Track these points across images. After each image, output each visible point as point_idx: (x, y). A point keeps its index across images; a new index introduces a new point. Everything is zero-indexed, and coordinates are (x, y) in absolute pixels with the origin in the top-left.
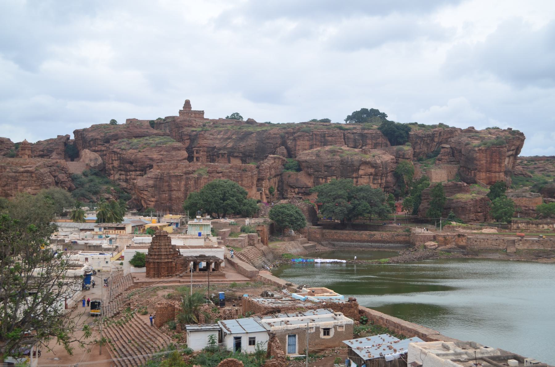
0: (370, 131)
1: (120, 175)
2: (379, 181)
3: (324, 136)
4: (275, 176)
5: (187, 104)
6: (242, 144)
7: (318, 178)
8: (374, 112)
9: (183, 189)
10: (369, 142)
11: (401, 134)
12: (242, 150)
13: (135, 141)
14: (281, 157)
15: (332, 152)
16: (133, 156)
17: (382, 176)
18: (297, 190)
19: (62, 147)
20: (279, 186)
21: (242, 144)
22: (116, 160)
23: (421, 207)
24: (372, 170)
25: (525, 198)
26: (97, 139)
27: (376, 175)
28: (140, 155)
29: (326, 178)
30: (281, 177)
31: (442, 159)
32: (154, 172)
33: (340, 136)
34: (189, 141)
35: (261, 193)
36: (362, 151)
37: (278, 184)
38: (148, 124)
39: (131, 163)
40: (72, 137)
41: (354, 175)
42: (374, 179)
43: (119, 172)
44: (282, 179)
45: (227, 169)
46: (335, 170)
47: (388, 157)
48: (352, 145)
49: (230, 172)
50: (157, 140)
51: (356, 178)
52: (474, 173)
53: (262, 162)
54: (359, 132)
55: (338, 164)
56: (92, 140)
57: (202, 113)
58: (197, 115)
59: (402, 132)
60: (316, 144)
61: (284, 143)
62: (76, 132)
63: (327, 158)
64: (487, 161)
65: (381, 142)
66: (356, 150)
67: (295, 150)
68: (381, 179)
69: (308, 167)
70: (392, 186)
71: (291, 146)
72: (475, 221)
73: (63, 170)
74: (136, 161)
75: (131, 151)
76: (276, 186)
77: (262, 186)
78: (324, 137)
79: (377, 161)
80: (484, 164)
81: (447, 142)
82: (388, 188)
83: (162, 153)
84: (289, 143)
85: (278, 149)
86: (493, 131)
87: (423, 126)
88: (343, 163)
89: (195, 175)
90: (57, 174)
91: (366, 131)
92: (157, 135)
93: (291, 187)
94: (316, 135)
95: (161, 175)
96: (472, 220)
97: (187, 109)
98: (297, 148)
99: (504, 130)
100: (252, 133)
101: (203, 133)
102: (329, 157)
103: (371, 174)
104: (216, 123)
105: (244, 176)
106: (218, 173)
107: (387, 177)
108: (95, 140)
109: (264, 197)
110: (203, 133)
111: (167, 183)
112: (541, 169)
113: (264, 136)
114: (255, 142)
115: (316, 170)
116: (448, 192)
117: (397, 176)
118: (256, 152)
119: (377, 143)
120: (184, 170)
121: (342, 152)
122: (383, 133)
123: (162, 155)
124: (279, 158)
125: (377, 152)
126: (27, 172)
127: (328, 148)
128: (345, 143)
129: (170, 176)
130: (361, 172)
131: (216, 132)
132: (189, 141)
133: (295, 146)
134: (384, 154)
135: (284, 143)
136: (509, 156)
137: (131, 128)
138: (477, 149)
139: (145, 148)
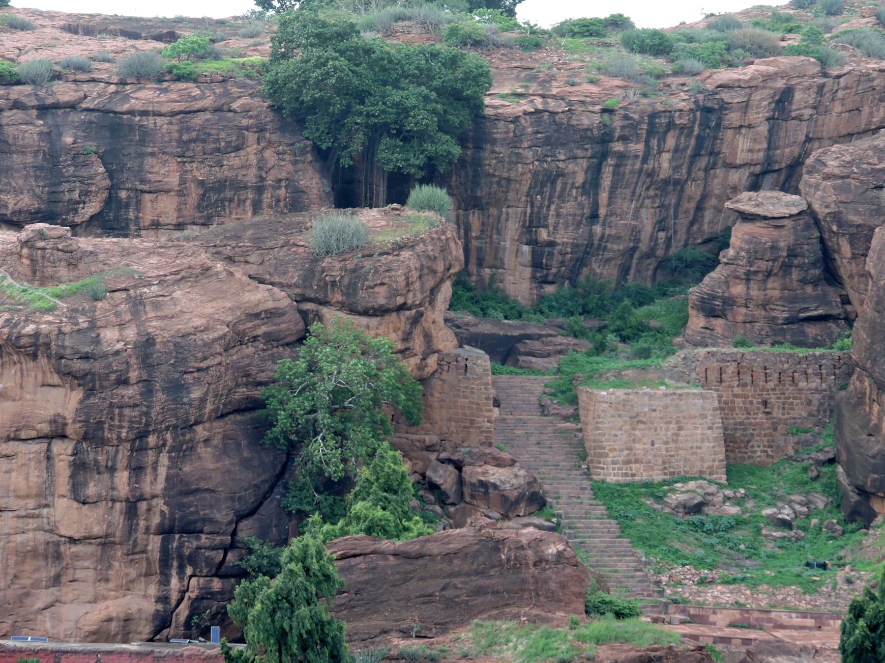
2: (122, 478)
11: (404, 111)
24: (65, 402)
31: (730, 302)
42: (79, 467)
54: (95, 95)
59: (410, 94)
68: (137, 470)
70: (223, 515)
79: (109, 335)
81: (789, 178)
82: (191, 530)
91: (145, 96)
107: (182, 451)
116: (428, 598)
119: (221, 185)
122: (277, 109)
125: (141, 257)
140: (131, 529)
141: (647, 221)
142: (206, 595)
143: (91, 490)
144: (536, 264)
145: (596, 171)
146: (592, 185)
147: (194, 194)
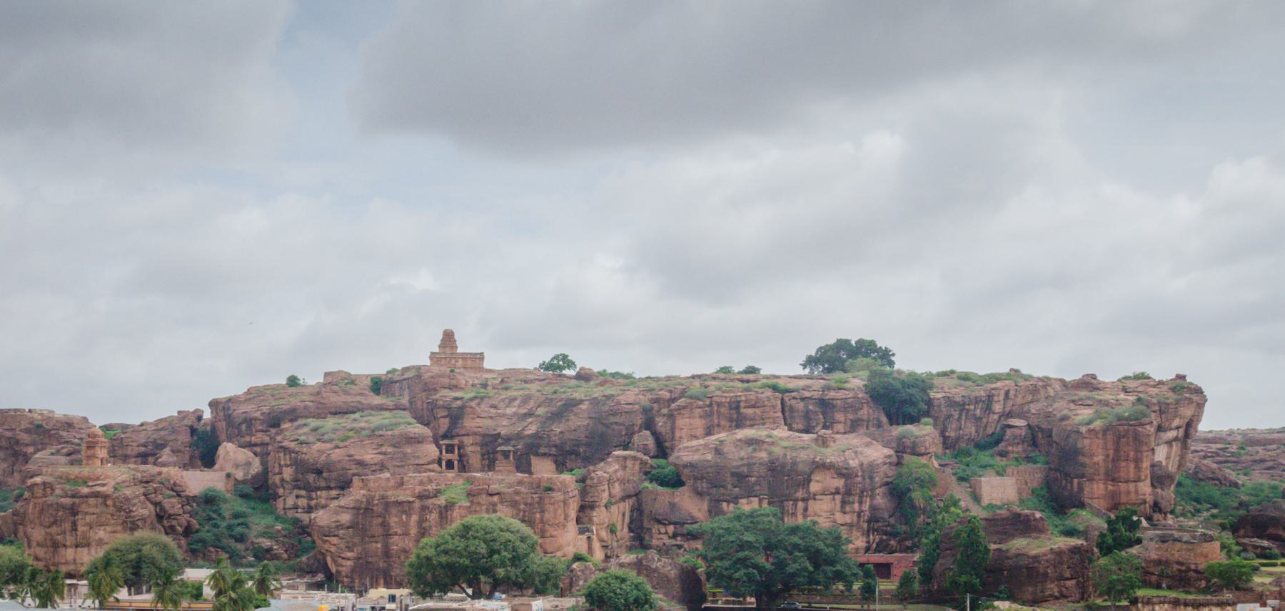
0: (841, 394)
1: (297, 497)
2: (856, 506)
3: (735, 406)
4: (623, 499)
5: (448, 338)
6: (557, 428)
7: (718, 501)
8: (865, 348)
9: (414, 531)
10: (840, 417)
12: (556, 439)
13: (330, 423)
14: (640, 455)
15: (750, 442)
16: (323, 458)
17: (861, 496)
18: (671, 529)
19: (185, 437)
20: (631, 522)
21: (557, 428)
22: (287, 466)
23: (938, 568)
24: (839, 483)
25: (1178, 545)
26: (256, 419)
27: (848, 492)
28: (336, 455)
29: (735, 500)
30: (638, 500)
31: (1007, 452)
32: (357, 494)
33: (774, 407)
34: (447, 420)
35: (589, 538)
36: (817, 440)
37: (631, 516)
38: (368, 382)
39: (319, 472)
40: (207, 415)
41: (800, 494)
42: (844, 503)
43: (296, 492)
44: (640, 504)
45: (510, 486)
46: (756, 483)
47: (877, 453)
48: (800, 427)
49: (517, 493)
50: (377, 420)
51: (803, 500)
52: (1079, 483)
53: (591, 468)
54: (817, 395)
55: (763, 471)
56: (245, 421)
57: (480, 357)
58: (469, 363)
60: (719, 426)
61: (649, 425)
62: (214, 404)
63: (736, 456)
64: (1108, 456)
65: (865, 417)
66: (806, 437)
67: (673, 439)
68: (861, 503)
69: (696, 478)
70: (886, 516)
71: (663, 430)
72: (1057, 598)
73: (177, 490)
74: (329, 466)
75: (319, 446)
76: (627, 520)
77: (591, 521)
78: (738, 408)
80: (1101, 463)
81: (1021, 415)
83: (383, 449)
84: (660, 423)
85: (636, 438)
86: (1131, 384)
87: (965, 377)
88: (775, 468)
89: (441, 501)
90: (160, 498)
91: (832, 394)
92: (381, 408)
93: (659, 522)
94: (719, 405)
95: (368, 501)
96: (1051, 596)
97: (448, 350)
98: (677, 434)
99: (1161, 383)
100: (581, 402)
101: (473, 404)
102: (742, 453)
103: (837, 492)
104: (506, 379)
105: (546, 501)
106: (492, 495)
107: (872, 497)
108: (249, 422)
109: (596, 545)
110: (473, 404)
111: (380, 520)
112: (1270, 464)
113: (606, 408)
114: (586, 422)
115: (717, 483)
117: (898, 494)
118: (588, 445)
120: (418, 489)
121: (773, 444)
123: (384, 454)
124: (635, 458)
125: (854, 440)
126: (96, 495)
127: (742, 434)
128: (785, 419)
129: (387, 505)
130: (814, 487)
131: (503, 400)
132: (447, 420)
133: (673, 429)
134: (867, 445)
135: (649, 425)
136: (1169, 443)
137: (325, 395)
138: (1083, 429)
139: (349, 438)
140: (859, 522)
141: (973, 429)
142: (881, 541)
143: (848, 509)
144: (944, 443)
145: (960, 415)
146: (959, 419)
147: (849, 423)
